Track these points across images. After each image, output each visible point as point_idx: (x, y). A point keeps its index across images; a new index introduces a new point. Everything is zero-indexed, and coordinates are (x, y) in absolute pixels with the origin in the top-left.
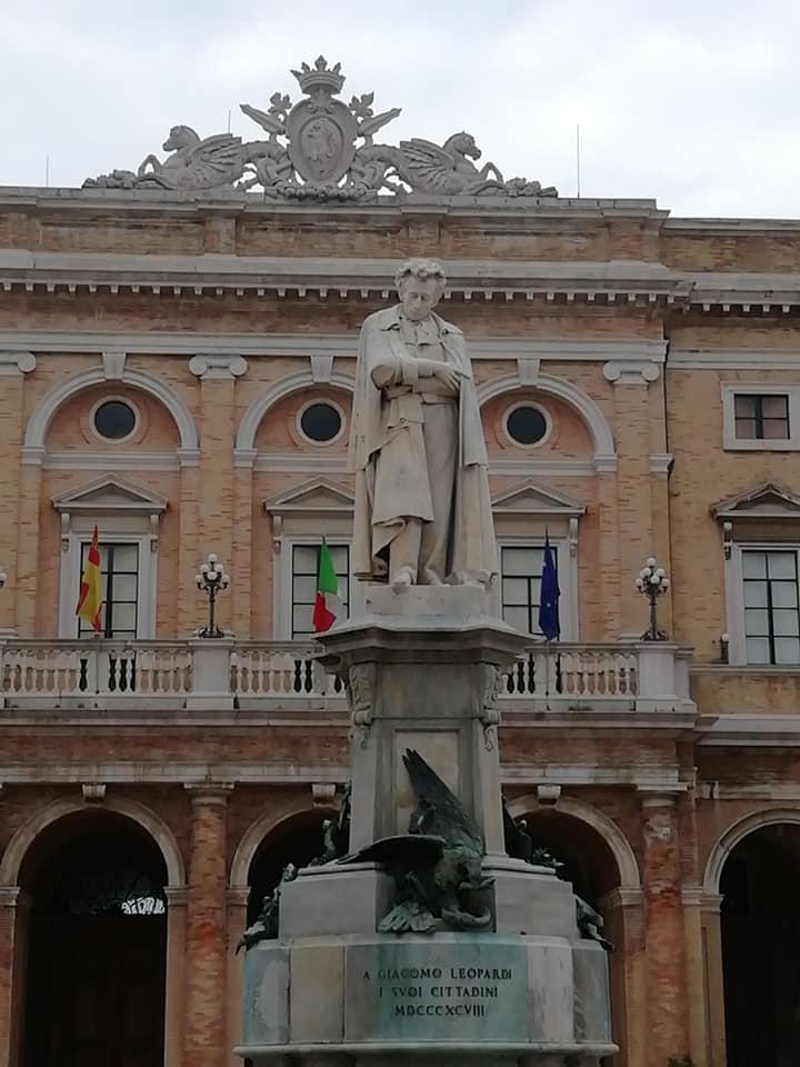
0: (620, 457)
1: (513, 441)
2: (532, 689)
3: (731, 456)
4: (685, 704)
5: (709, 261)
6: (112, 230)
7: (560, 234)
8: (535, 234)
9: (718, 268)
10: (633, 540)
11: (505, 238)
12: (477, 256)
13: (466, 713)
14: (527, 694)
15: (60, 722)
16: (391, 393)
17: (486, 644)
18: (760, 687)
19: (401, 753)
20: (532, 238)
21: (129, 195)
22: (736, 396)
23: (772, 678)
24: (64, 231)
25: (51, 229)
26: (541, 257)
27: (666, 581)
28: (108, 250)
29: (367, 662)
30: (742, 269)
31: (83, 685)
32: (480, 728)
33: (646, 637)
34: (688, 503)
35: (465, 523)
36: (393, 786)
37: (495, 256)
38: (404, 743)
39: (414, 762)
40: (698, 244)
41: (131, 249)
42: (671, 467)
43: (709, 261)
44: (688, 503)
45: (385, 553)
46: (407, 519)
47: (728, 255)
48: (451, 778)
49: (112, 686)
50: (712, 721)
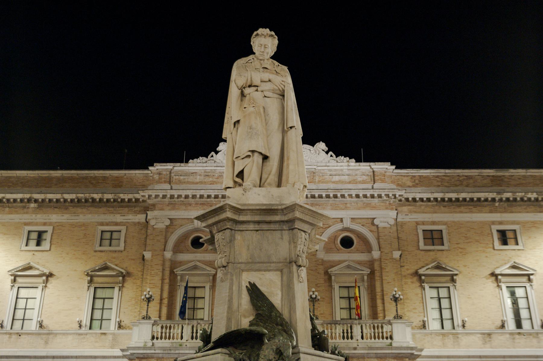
0: (382, 252)
1: (342, 248)
2: (352, 338)
3: (423, 252)
4: (412, 344)
5: (410, 184)
6: (198, 177)
7: (356, 175)
8: (348, 175)
9: (414, 186)
10: (388, 283)
11: (337, 177)
12: (327, 182)
13: (286, 259)
14: (350, 340)
15: (172, 352)
16: (247, 91)
17: (298, 214)
18: (441, 337)
19: (245, 284)
20: (347, 176)
21: (205, 165)
22: (423, 230)
23: (444, 335)
24: (182, 177)
25: (177, 177)
26: (350, 183)
27: (402, 297)
28: (197, 183)
29: (225, 229)
30: (422, 186)
31: (182, 338)
32: (295, 267)
33: (395, 318)
34: (407, 269)
35: (288, 159)
36: (239, 305)
37: (334, 182)
38: (247, 278)
39: (254, 291)
40: (406, 178)
41: (205, 183)
42: (400, 256)
43: (410, 184)
44: (407, 269)
45: (241, 174)
46: (253, 151)
47: (417, 182)
48: (277, 299)
49: (192, 338)
50: (421, 350)
